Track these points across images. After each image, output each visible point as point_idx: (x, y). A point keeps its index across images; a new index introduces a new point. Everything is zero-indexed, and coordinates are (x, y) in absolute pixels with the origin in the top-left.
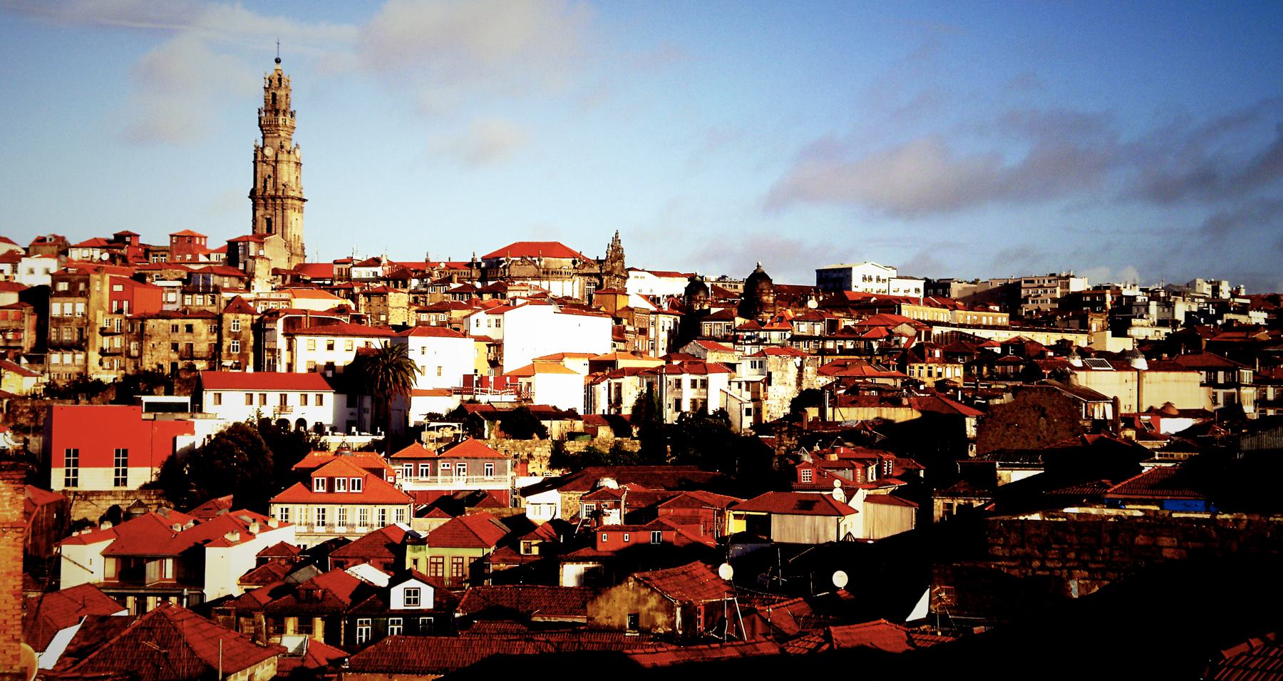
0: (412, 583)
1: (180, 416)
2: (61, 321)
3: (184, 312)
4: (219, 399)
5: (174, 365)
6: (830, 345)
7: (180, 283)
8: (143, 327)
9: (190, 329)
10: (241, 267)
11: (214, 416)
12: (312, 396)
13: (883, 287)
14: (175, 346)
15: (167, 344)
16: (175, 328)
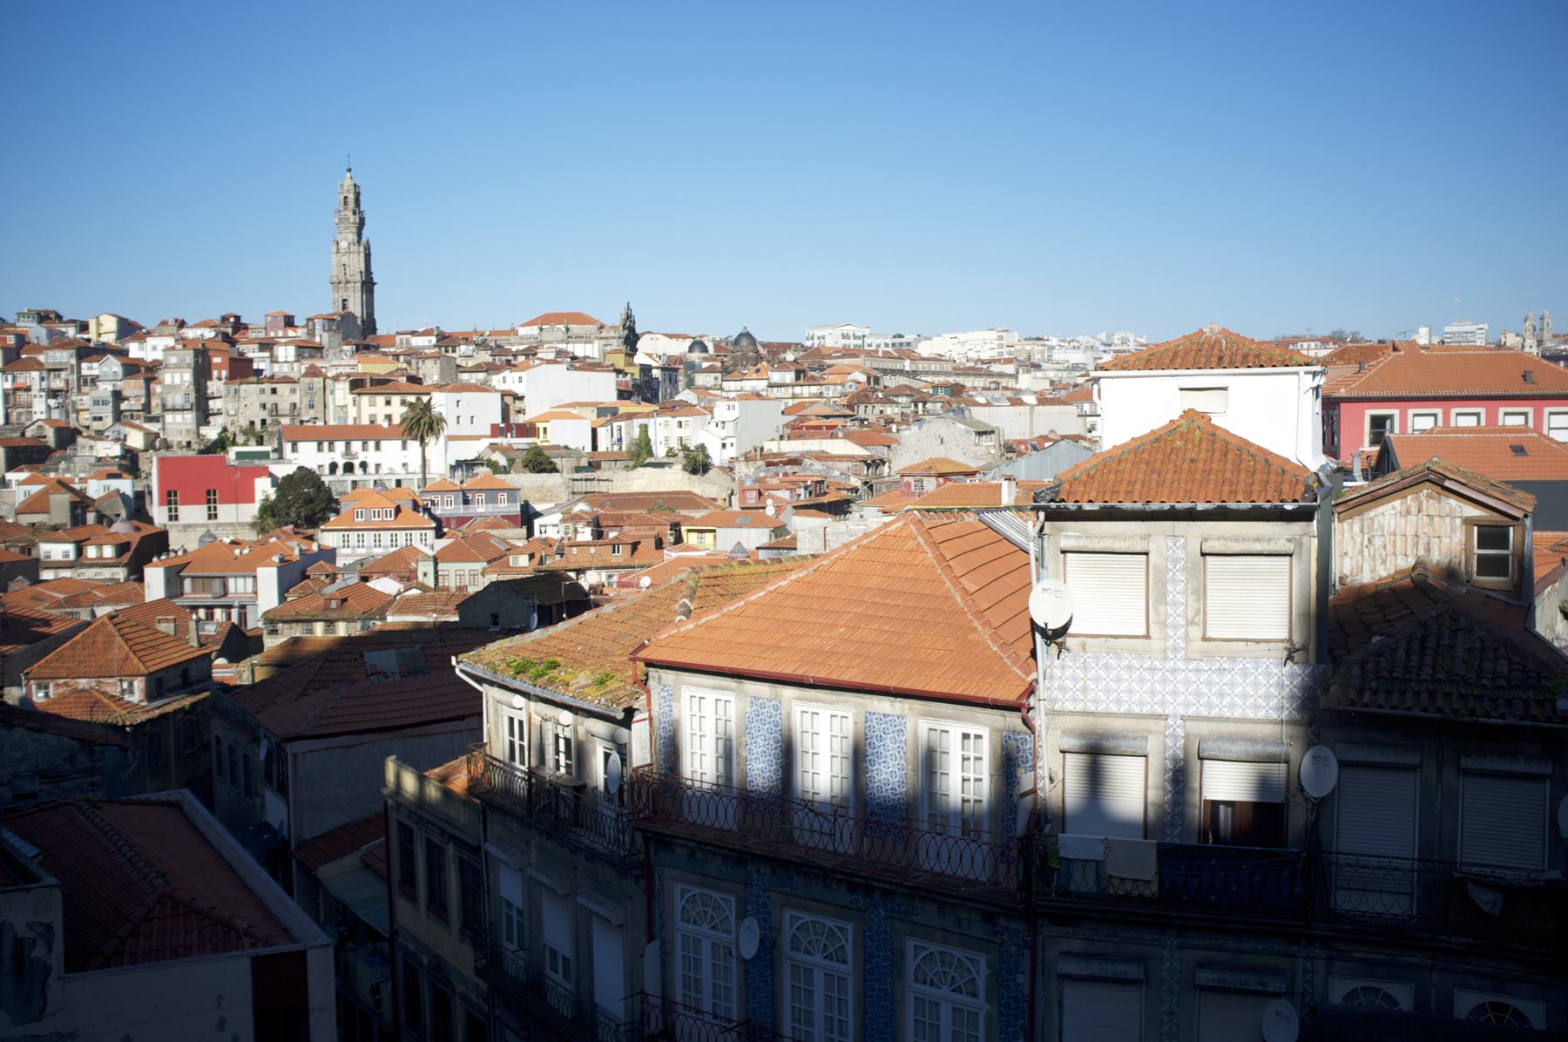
0: (415, 592)
1: (263, 462)
2: (173, 387)
3: (272, 377)
4: (294, 450)
5: (264, 422)
6: (798, 390)
7: (267, 354)
8: (237, 391)
9: (274, 391)
10: (317, 339)
11: (290, 462)
12: (371, 444)
13: (859, 342)
14: (264, 406)
15: (257, 405)
16: (262, 391)
